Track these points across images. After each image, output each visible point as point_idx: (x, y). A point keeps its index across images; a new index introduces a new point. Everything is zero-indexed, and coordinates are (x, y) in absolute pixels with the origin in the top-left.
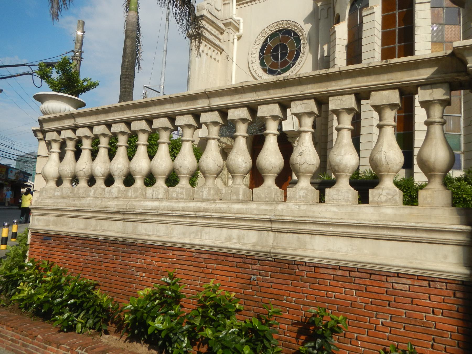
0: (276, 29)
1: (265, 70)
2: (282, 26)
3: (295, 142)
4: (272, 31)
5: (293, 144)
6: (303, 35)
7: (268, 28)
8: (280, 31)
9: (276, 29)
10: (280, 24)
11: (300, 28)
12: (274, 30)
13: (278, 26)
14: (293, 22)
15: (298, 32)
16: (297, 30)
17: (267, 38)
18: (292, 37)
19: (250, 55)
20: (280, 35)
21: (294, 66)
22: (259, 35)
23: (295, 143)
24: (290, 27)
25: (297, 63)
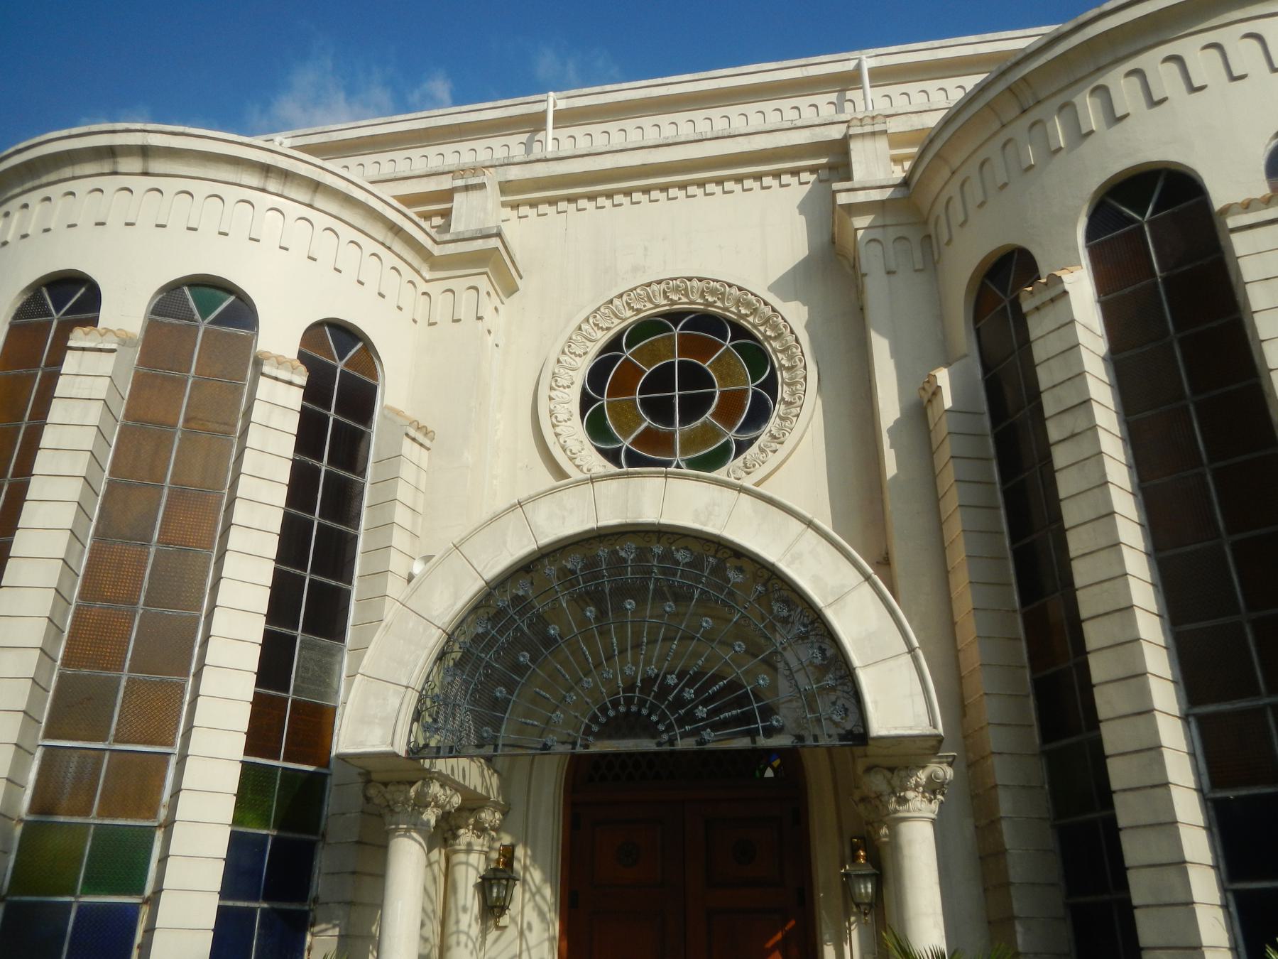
0: (657, 306)
1: (613, 457)
2: (684, 300)
3: (910, 794)
4: (639, 311)
5: (893, 806)
6: (779, 336)
7: (625, 298)
8: (675, 316)
9: (657, 306)
10: (677, 290)
11: (768, 311)
12: (648, 310)
13: (666, 297)
14: (730, 286)
15: (755, 326)
16: (751, 319)
17: (620, 335)
18: (728, 344)
19: (544, 392)
20: (677, 331)
21: (754, 449)
22: (587, 320)
23: (903, 801)
24: (719, 304)
25: (764, 439)
